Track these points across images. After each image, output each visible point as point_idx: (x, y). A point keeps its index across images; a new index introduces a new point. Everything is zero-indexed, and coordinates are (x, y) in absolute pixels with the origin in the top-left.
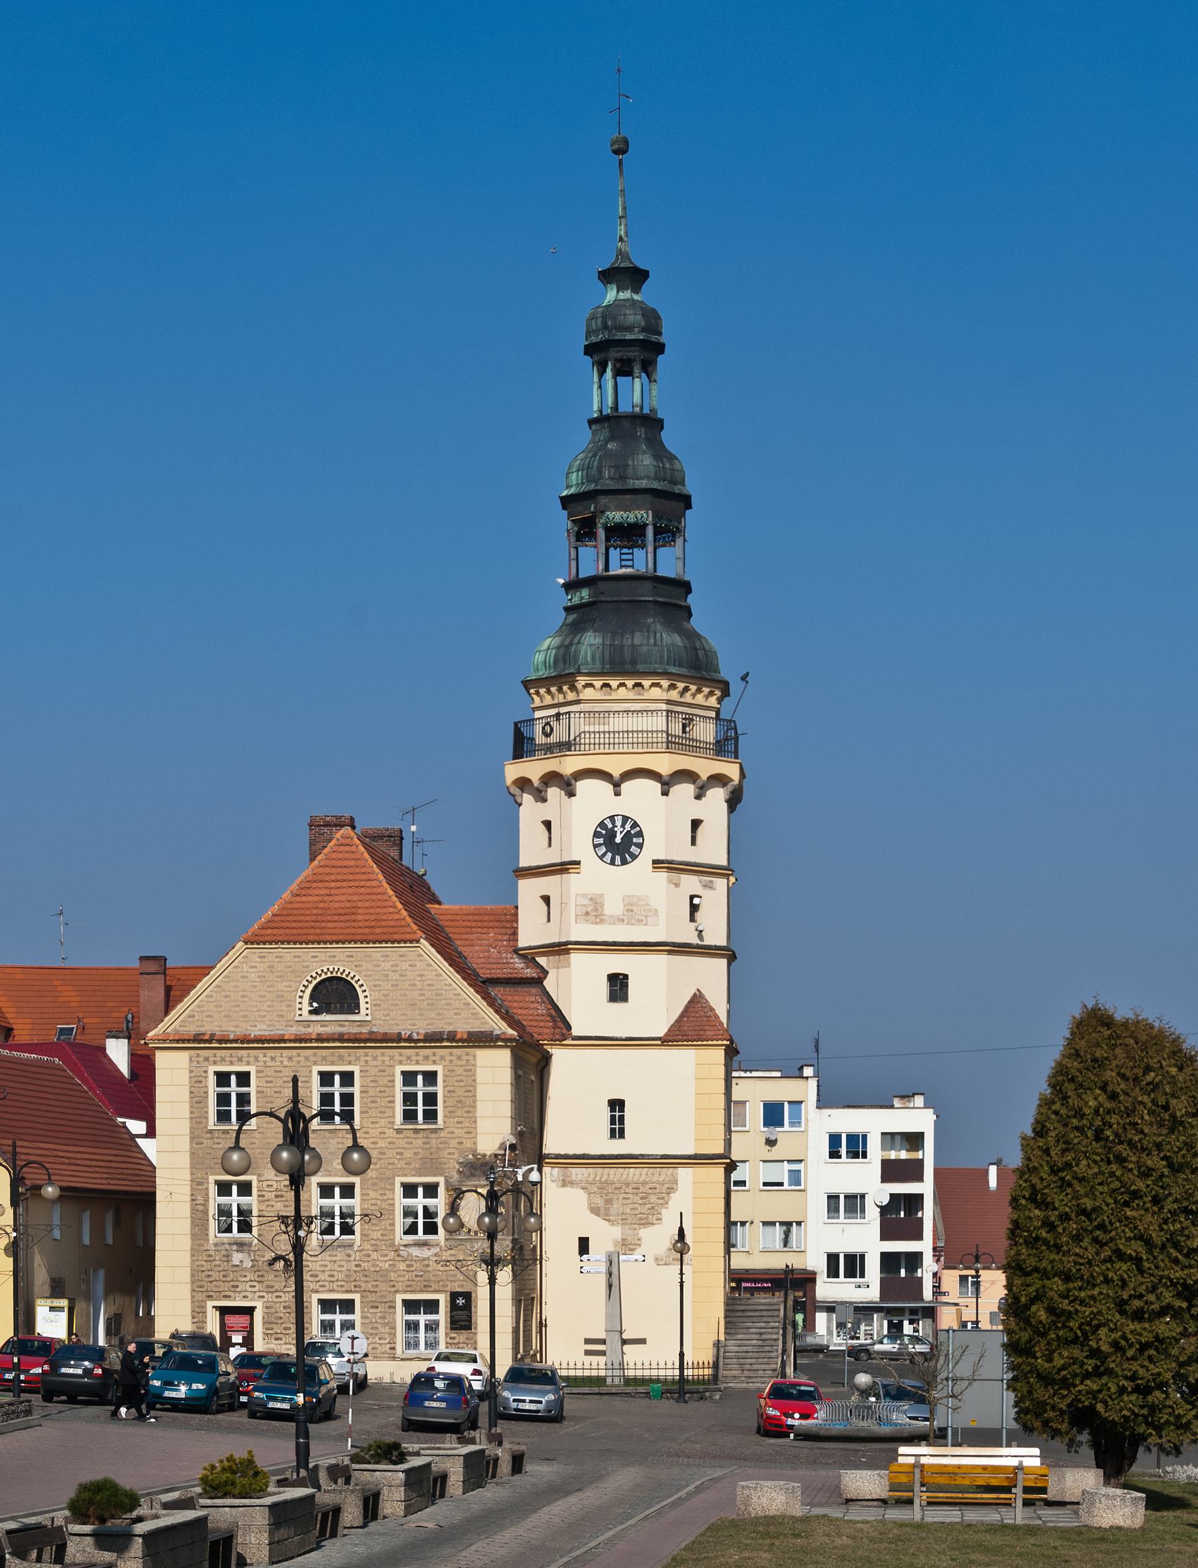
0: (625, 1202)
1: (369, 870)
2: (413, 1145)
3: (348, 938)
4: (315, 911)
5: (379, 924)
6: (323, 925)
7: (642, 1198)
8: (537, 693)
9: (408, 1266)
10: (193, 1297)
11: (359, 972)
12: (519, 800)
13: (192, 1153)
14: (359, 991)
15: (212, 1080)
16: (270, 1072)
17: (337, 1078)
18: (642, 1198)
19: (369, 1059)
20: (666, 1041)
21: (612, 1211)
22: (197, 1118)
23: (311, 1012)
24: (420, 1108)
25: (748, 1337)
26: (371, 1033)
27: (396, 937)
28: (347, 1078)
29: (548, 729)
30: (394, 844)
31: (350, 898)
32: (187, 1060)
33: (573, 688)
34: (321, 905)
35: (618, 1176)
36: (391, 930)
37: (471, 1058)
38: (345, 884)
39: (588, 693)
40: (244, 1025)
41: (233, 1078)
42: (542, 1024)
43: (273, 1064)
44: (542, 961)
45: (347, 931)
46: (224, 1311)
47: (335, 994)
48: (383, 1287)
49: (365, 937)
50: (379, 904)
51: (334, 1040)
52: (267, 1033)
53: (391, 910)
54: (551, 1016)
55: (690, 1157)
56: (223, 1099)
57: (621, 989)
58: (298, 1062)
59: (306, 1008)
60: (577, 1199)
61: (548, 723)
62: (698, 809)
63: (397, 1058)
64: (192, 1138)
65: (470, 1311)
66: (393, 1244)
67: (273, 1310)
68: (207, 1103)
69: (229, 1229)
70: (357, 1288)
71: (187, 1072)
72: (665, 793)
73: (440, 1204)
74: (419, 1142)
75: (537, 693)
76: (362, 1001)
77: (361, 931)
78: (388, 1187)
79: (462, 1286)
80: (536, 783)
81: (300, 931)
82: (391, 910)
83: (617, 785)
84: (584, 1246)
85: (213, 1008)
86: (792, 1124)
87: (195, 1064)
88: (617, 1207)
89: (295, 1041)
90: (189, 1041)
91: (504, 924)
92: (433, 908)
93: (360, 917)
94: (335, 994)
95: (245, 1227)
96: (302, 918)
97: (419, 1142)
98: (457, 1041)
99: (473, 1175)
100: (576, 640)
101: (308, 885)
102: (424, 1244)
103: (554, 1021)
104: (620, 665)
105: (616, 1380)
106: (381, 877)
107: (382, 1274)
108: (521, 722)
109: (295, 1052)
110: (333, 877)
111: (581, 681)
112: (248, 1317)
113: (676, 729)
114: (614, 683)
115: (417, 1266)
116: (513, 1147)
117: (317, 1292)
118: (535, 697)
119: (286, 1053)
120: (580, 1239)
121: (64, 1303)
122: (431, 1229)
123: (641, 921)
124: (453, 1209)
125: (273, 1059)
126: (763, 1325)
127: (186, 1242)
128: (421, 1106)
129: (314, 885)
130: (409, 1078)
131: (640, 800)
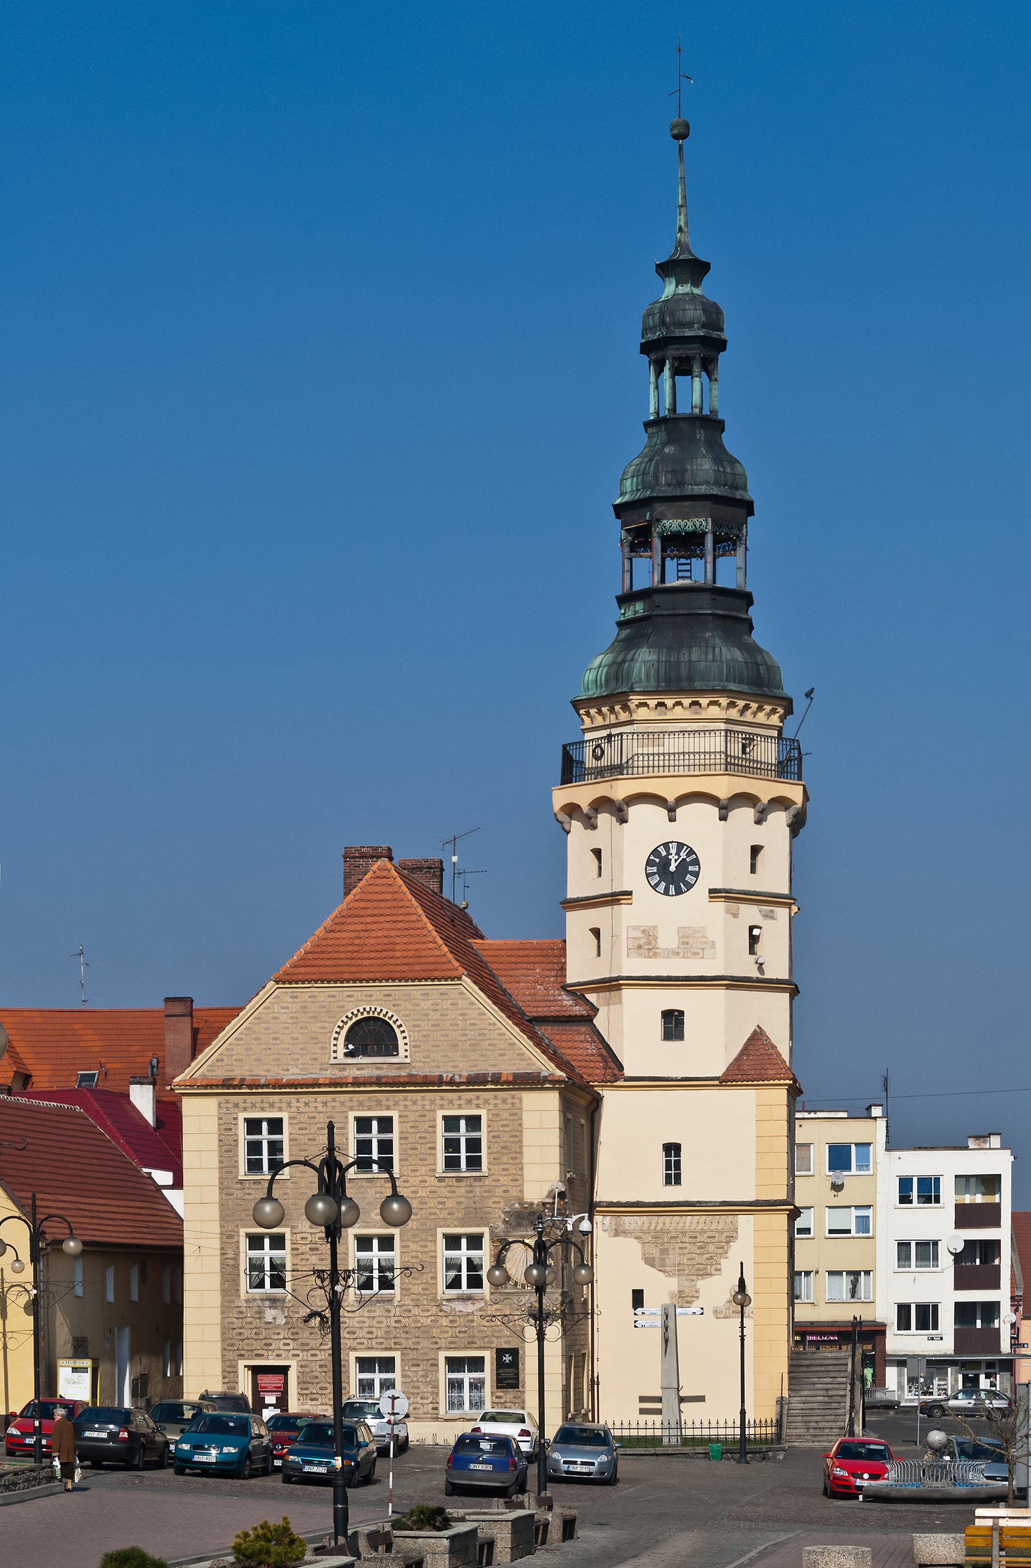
1: (407, 904)
2: (457, 1193)
3: (385, 975)
4: (350, 948)
5: (418, 960)
6: (359, 962)
7: (700, 1248)
8: (588, 714)
9: (451, 1321)
10: (223, 1356)
11: (398, 1012)
12: (567, 827)
13: (221, 1205)
14: (397, 1031)
15: (242, 1128)
16: (303, 1118)
17: (375, 1124)
18: (700, 1248)
19: (408, 1103)
20: (724, 1081)
21: (668, 1262)
22: (227, 1168)
23: (346, 1055)
24: (463, 1154)
25: (813, 1393)
26: (411, 1076)
27: (436, 974)
28: (386, 1124)
29: (598, 751)
30: (434, 875)
31: (386, 933)
32: (216, 1106)
33: (626, 708)
34: (357, 942)
35: (674, 1225)
36: (432, 967)
37: (516, 1101)
38: (382, 919)
39: (642, 713)
40: (275, 1069)
41: (265, 1125)
42: (592, 1064)
43: (307, 1109)
44: (592, 997)
45: (384, 968)
46: (257, 1371)
47: (372, 1036)
48: (425, 1344)
49: (403, 975)
50: (418, 939)
51: (371, 1084)
52: (300, 1077)
53: (431, 945)
54: (602, 1056)
55: (750, 1204)
56: (254, 1148)
57: (676, 1026)
58: (333, 1107)
59: (341, 1050)
60: (631, 1248)
61: (599, 746)
62: (758, 835)
63: (438, 1102)
64: (221, 1189)
65: (517, 1368)
66: (435, 1299)
67: (307, 1370)
68: (237, 1151)
69: (261, 1285)
70: (397, 1346)
71: (216, 1118)
72: (723, 818)
73: (485, 1255)
74: (462, 1190)
75: (588, 714)
76: (401, 1042)
77: (399, 968)
78: (430, 1238)
79: (508, 1342)
80: (585, 809)
81: (334, 969)
82: (431, 945)
83: (671, 810)
84: (638, 1298)
85: (243, 1052)
86: (860, 1167)
87: (224, 1110)
88: (673, 1258)
89: (330, 1085)
90: (217, 1086)
91: (551, 959)
92: (475, 943)
93: (398, 954)
94: (372, 1036)
95: (278, 1281)
96: (336, 955)
97: (463, 1190)
98: (502, 1084)
99: (519, 1225)
100: (629, 657)
101: (343, 920)
102: (469, 1298)
103: (605, 1061)
104: (675, 683)
105: (673, 1440)
106: (420, 911)
107: (425, 1330)
108: (570, 744)
109: (329, 1097)
110: (369, 912)
111: (635, 700)
112: (282, 1377)
113: (736, 749)
114: (670, 703)
115: (460, 1321)
116: (562, 1195)
117: (355, 1349)
118: (585, 717)
119: (320, 1098)
120: (634, 1291)
121: (87, 1363)
122: (475, 1282)
123: (698, 954)
124: (499, 1261)
125: (306, 1104)
126: (830, 1380)
127: (216, 1299)
128: (463, 1153)
129: (349, 920)
130: (451, 1123)
131: (697, 825)
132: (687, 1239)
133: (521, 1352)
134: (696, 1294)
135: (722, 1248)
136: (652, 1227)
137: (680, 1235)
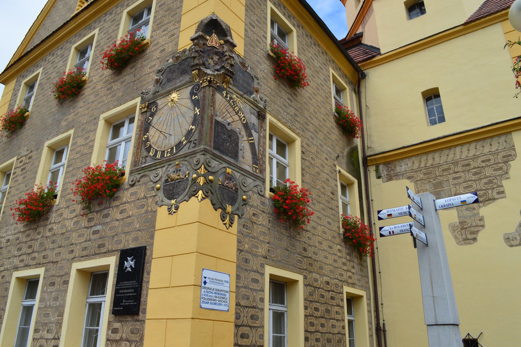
0: (456, 182)
18: (475, 174)
117: (16, 268)
132: (460, 169)
133: (148, 252)
134: (480, 223)
135: (501, 169)
136: (423, 165)
137: (452, 166)
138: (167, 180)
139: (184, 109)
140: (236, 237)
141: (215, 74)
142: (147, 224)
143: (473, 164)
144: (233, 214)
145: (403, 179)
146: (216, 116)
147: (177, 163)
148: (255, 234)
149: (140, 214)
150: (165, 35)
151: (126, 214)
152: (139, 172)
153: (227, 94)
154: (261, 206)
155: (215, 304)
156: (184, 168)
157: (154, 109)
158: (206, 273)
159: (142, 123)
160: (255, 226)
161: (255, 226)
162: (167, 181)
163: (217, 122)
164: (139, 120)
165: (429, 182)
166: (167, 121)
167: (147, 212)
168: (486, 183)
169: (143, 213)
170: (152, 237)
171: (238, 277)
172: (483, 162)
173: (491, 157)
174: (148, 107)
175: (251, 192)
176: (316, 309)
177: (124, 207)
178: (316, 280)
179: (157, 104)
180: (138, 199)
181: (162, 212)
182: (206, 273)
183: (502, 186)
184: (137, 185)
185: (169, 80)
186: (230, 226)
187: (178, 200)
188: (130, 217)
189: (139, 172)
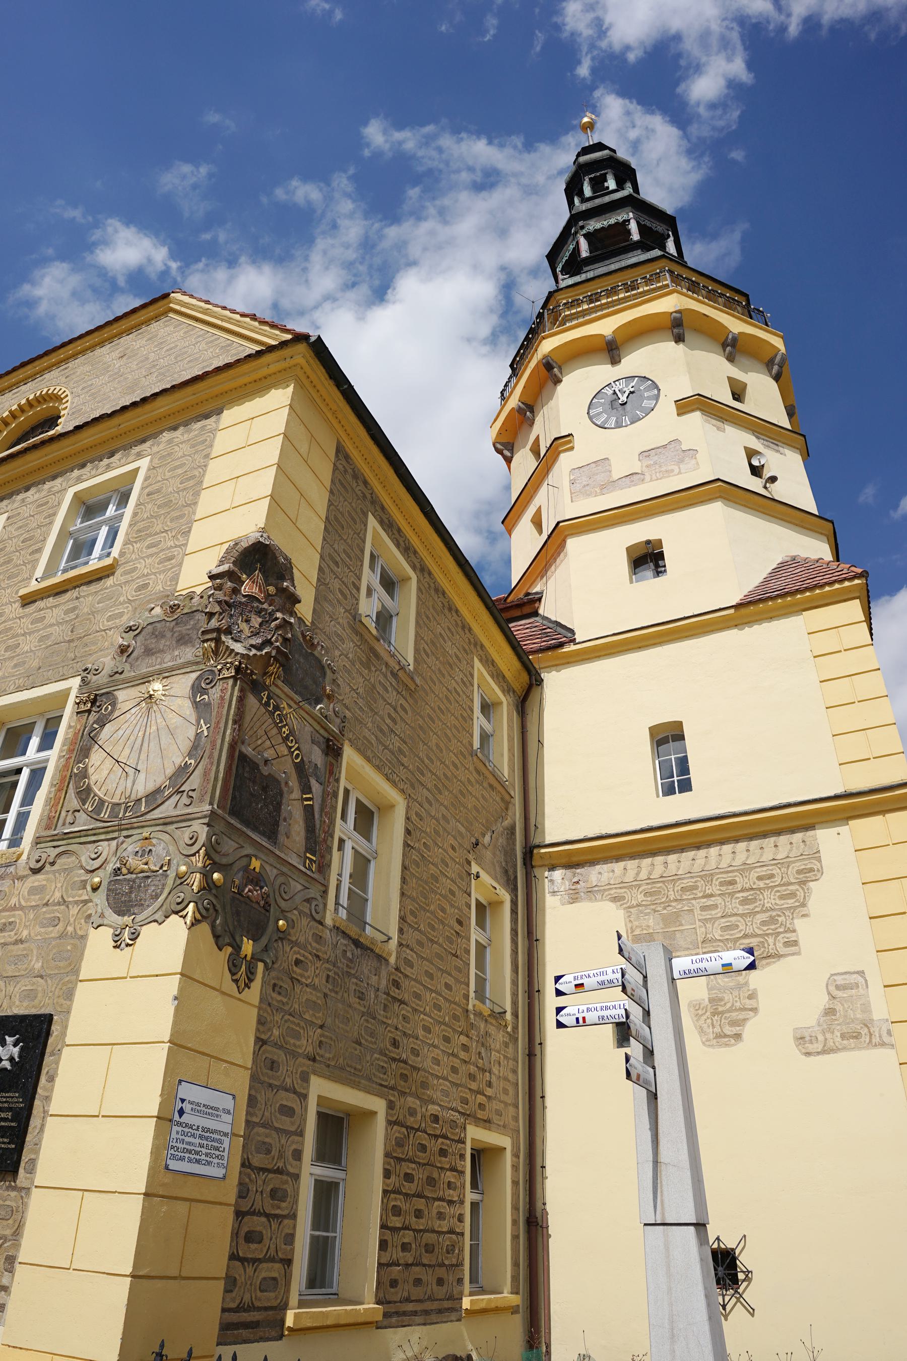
0: (707, 915)
7: (745, 901)
18: (745, 901)
79: (30, 995)
132: (715, 889)
134: (749, 1003)
135: (793, 895)
136: (643, 875)
137: (701, 883)
138: (119, 869)
139: (174, 720)
140: (256, 1010)
141: (251, 654)
142: (62, 964)
143: (741, 882)
144: (255, 958)
145: (602, 900)
146: (243, 743)
147: (146, 835)
148: (297, 1006)
149: (45, 939)
150: (151, 555)
151: (12, 933)
152: (55, 843)
153: (269, 698)
154: (314, 944)
155: (198, 1162)
156: (159, 849)
157: (107, 709)
158: (185, 1091)
159: (76, 734)
160: (298, 988)
161: (298, 988)
162: (117, 872)
163: (243, 757)
164: (70, 727)
165: (655, 911)
166: (132, 738)
167: (62, 935)
168: (764, 923)
169: (53, 938)
170: (69, 995)
171: (252, 1101)
172: (760, 878)
173: (776, 871)
174: (93, 703)
175: (295, 912)
176: (408, 1177)
177: (10, 916)
178: (412, 1112)
179: (116, 698)
180: (47, 904)
181: (100, 940)
182: (185, 1091)
183: (794, 931)
184: (47, 872)
185: (148, 652)
186: (247, 986)
187: (139, 918)
188: (21, 941)
189: (55, 843)
